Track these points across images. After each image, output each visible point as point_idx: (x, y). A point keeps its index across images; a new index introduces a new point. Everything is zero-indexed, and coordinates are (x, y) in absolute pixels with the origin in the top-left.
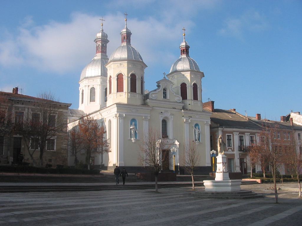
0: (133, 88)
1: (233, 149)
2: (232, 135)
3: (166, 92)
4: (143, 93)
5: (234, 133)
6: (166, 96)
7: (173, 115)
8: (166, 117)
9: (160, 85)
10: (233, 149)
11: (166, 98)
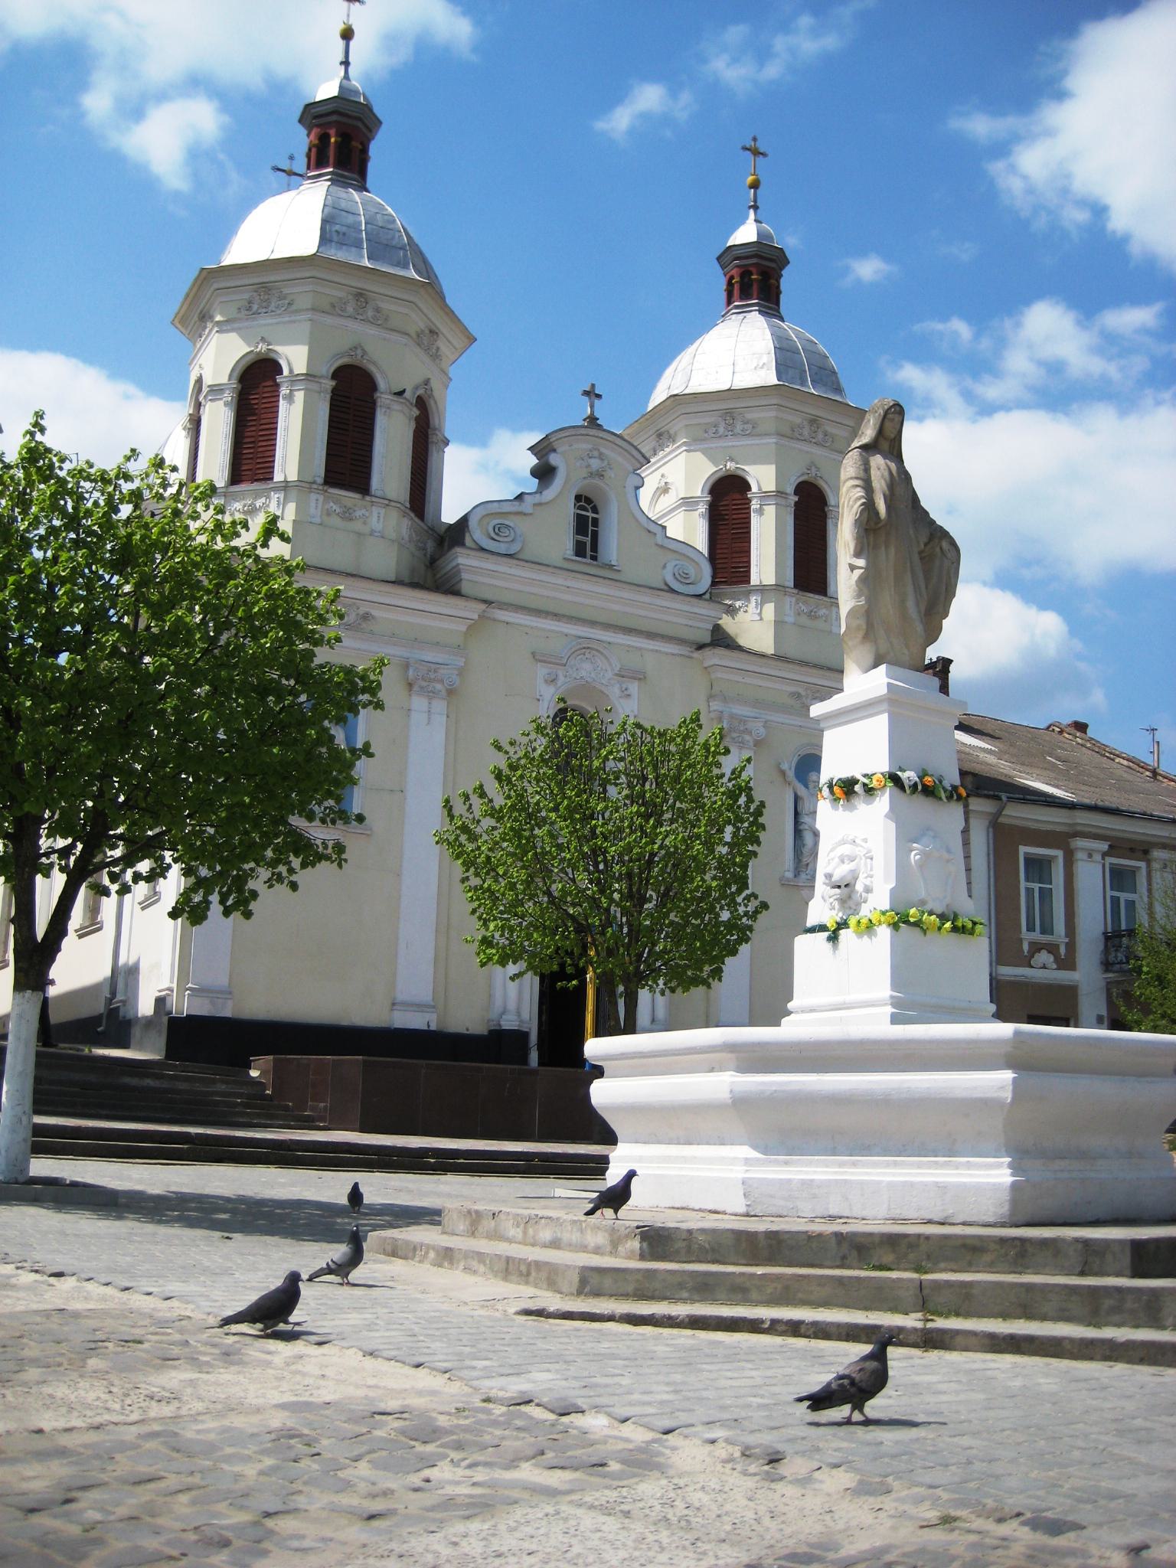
0: (346, 462)
1: (1062, 950)
2: (1059, 854)
3: (595, 522)
4: (429, 509)
5: (1080, 843)
6: (595, 547)
7: (640, 677)
8: (586, 688)
9: (554, 459)
10: (1062, 950)
11: (594, 558)
